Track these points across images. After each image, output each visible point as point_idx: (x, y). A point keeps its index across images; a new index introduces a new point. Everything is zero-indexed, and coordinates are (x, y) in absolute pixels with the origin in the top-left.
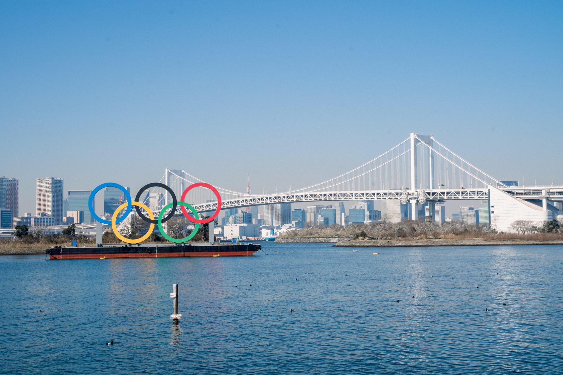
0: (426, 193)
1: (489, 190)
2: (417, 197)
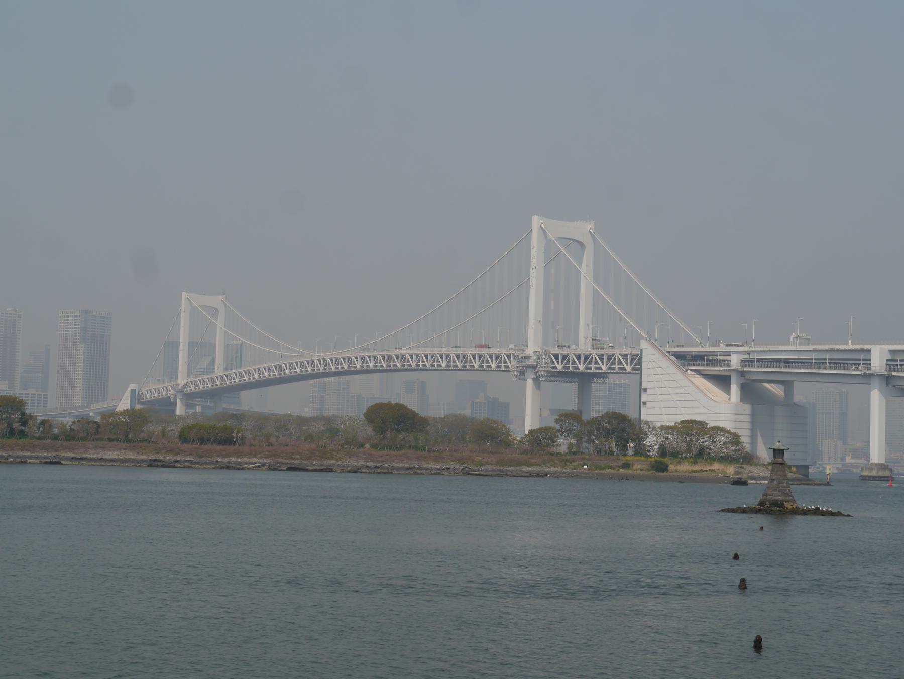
0: (552, 354)
1: (642, 350)
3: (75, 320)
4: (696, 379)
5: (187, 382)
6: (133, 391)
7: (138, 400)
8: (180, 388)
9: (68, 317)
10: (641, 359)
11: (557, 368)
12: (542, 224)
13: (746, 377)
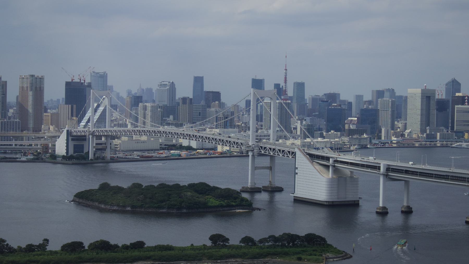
0: (260, 146)
2: (253, 150)
3: (27, 80)
4: (317, 166)
5: (94, 131)
6: (68, 131)
7: (70, 135)
8: (91, 132)
9: (23, 78)
10: (295, 154)
11: (261, 152)
12: (255, 92)
13: (336, 168)
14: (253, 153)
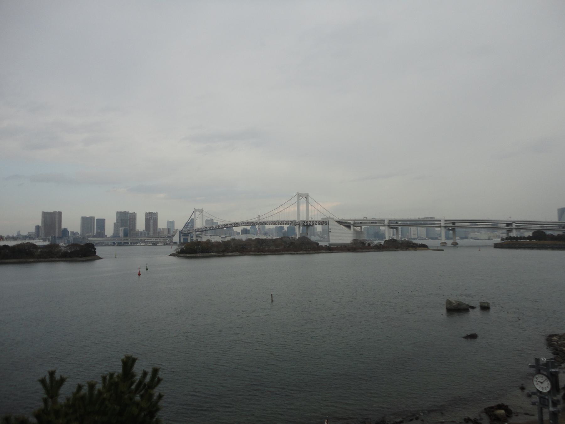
6: (180, 231)
14: (299, 226)
